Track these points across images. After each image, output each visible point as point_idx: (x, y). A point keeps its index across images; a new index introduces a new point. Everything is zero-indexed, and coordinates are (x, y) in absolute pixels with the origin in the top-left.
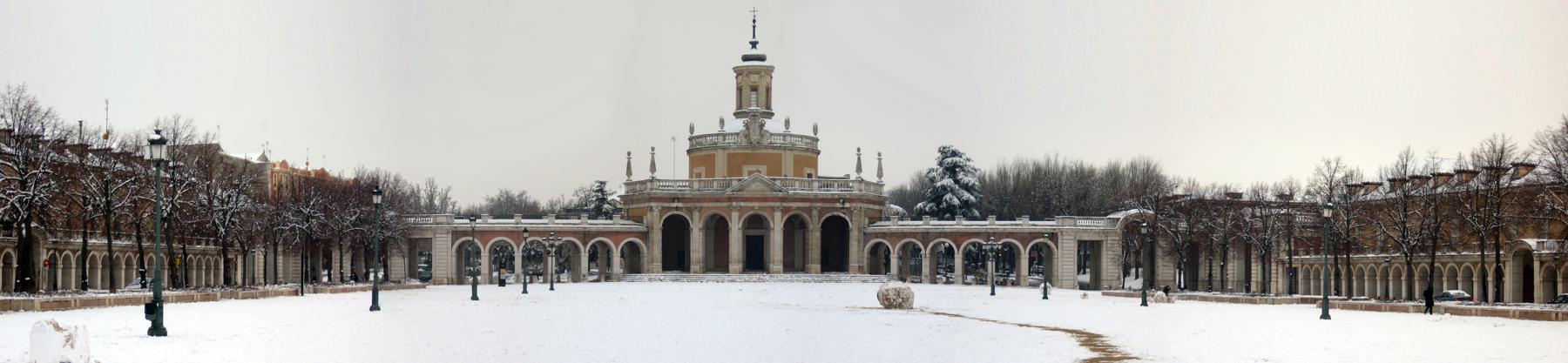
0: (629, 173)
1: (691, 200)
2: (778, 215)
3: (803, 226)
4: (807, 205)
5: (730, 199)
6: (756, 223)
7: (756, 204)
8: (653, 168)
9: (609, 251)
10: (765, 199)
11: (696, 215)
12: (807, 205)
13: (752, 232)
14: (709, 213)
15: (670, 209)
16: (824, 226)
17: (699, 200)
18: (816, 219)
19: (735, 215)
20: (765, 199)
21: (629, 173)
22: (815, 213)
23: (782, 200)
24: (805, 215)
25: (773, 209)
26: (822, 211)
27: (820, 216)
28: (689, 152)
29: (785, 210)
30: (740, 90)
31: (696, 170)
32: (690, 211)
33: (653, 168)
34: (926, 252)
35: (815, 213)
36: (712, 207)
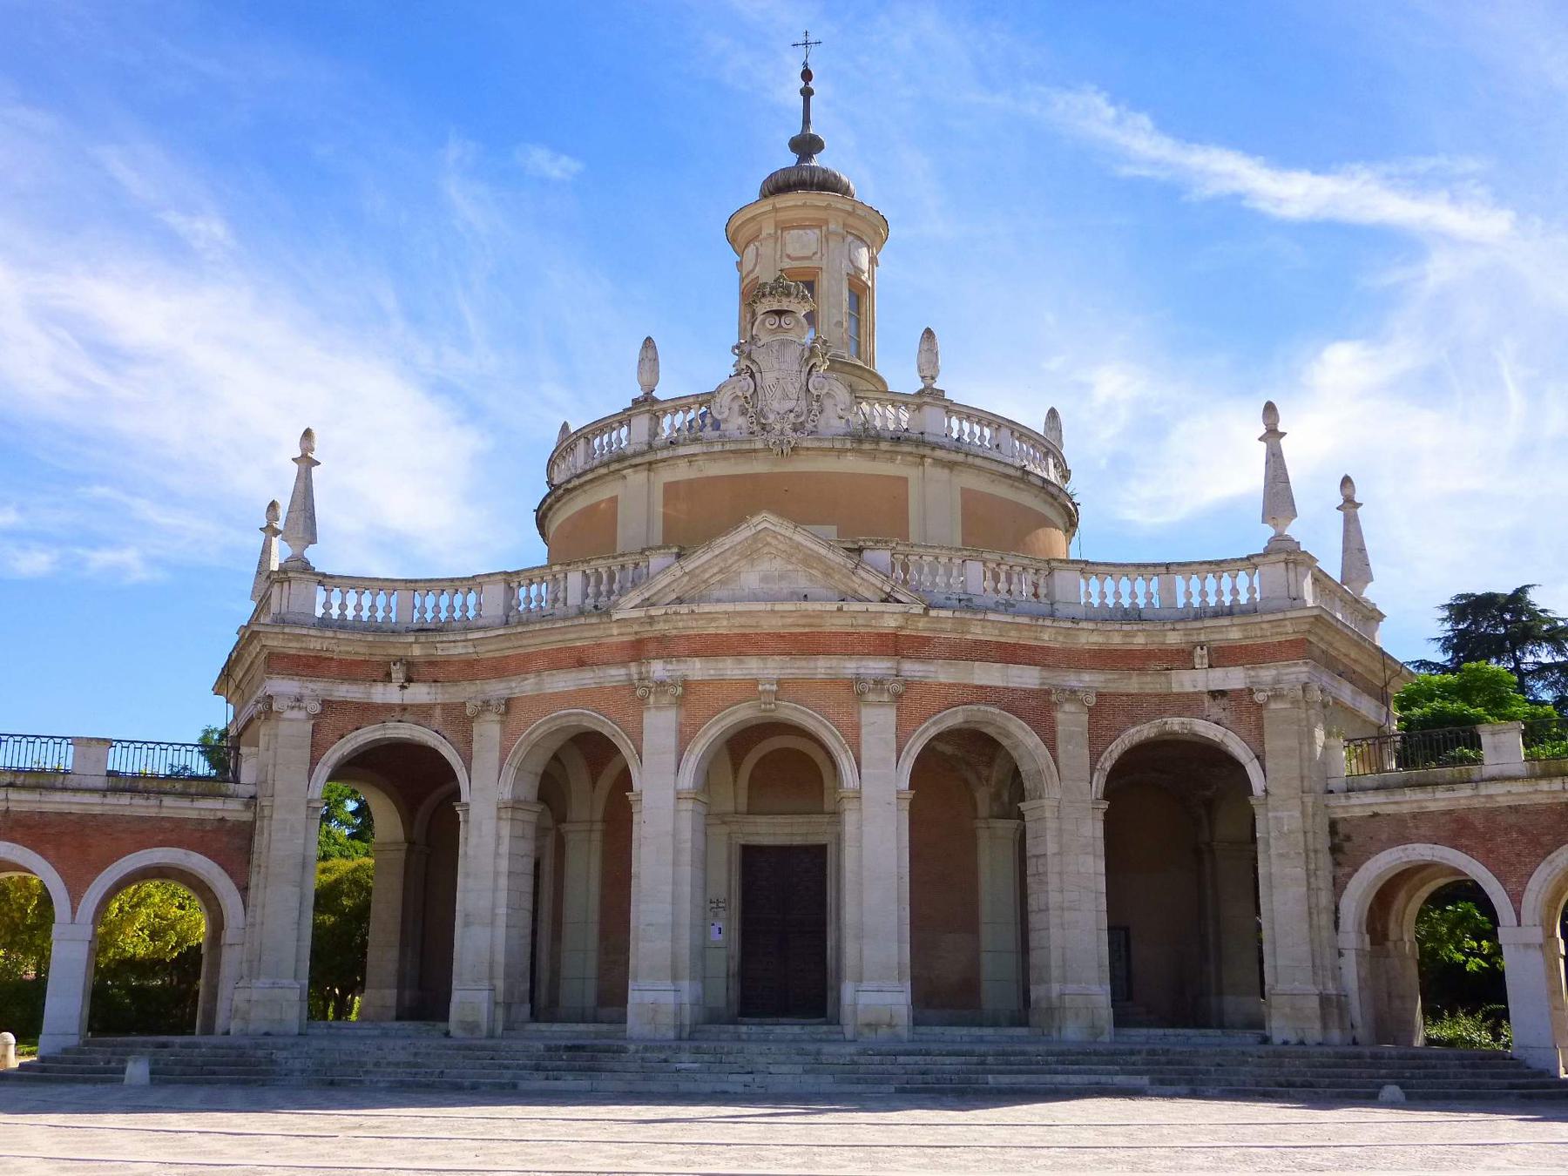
1: (470, 669)
2: (878, 721)
3: (1015, 792)
4: (1026, 677)
5: (638, 650)
6: (776, 764)
7: (766, 669)
10: (807, 644)
12: (1026, 677)
13: (773, 831)
14: (537, 727)
15: (369, 712)
16: (1113, 790)
17: (501, 669)
18: (1075, 750)
19: (660, 725)
20: (807, 644)
22: (1071, 721)
23: (894, 645)
24: (1023, 739)
25: (856, 689)
27: (1097, 742)
32: (460, 721)
35: (1071, 721)
36: (562, 695)
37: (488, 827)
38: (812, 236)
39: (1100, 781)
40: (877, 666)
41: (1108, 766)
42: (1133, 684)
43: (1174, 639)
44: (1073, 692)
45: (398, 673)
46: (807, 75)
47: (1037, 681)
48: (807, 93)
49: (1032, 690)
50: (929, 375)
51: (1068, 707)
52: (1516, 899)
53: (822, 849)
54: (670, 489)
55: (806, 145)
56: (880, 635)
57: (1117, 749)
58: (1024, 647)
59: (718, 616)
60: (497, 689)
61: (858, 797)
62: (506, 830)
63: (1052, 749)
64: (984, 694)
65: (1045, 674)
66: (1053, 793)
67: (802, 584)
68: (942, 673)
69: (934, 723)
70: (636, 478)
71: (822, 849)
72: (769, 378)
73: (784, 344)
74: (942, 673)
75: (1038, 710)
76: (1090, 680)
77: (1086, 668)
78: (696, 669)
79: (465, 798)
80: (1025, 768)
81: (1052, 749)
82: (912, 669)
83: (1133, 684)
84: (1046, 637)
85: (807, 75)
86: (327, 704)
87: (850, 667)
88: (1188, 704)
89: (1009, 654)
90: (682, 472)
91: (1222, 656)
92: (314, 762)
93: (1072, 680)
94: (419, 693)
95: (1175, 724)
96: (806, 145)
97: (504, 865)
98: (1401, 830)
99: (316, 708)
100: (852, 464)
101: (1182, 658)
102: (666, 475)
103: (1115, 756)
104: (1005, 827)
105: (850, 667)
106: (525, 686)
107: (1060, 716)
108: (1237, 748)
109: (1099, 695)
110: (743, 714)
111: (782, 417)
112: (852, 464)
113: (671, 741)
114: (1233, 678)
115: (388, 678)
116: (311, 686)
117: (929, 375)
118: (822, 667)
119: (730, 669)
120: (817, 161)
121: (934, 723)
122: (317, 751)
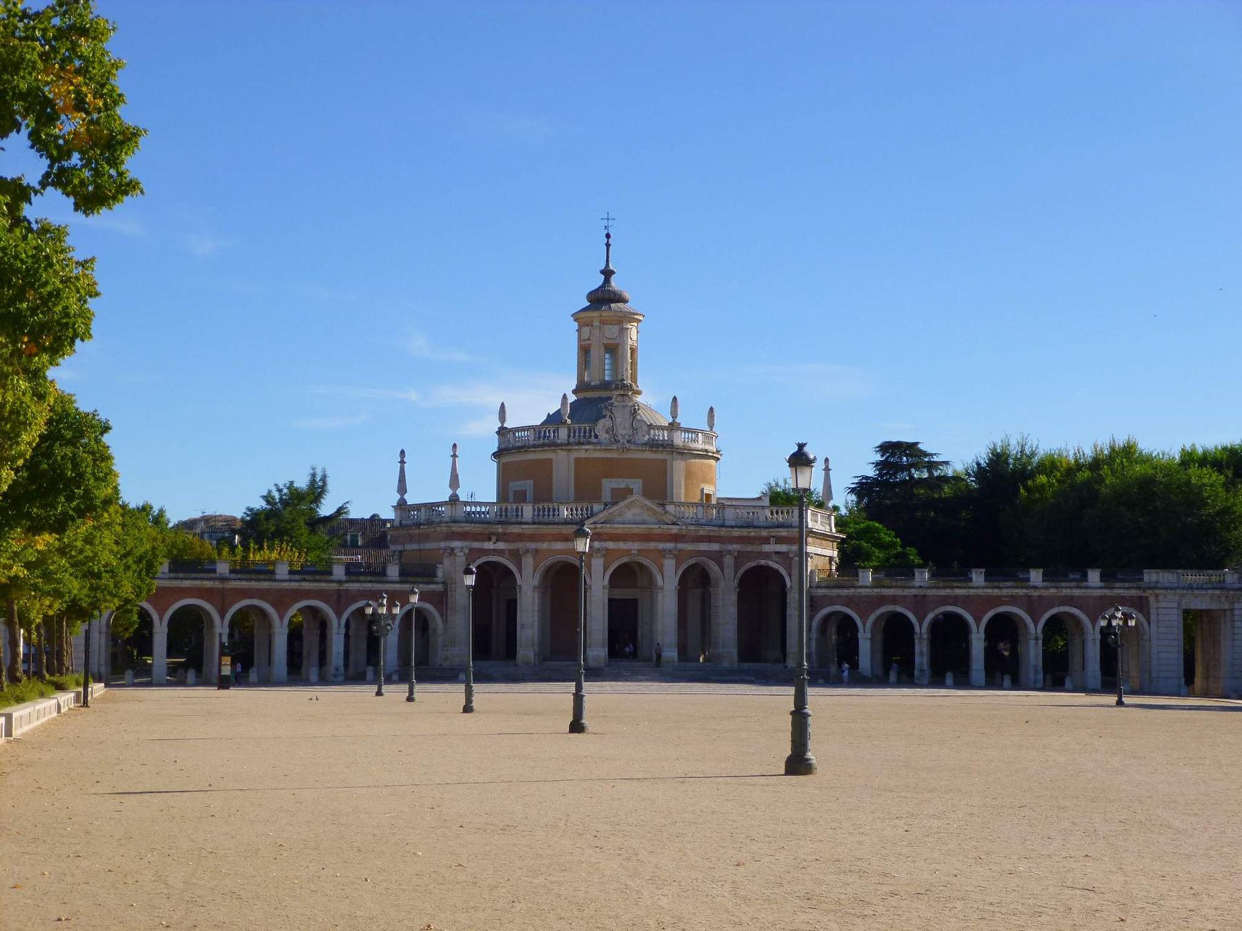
0: (402, 488)
2: (669, 564)
4: (715, 547)
6: (628, 575)
7: (634, 546)
8: (454, 481)
9: (323, 625)
11: (528, 562)
12: (715, 547)
13: (621, 594)
16: (742, 583)
17: (532, 538)
18: (729, 571)
20: (647, 537)
21: (402, 488)
22: (728, 561)
24: (714, 567)
25: (663, 553)
26: (740, 558)
27: (737, 566)
28: (496, 455)
29: (679, 556)
30: (584, 351)
31: (515, 486)
32: (516, 556)
33: (454, 481)
34: (922, 629)
35: (728, 561)
37: (530, 593)
38: (615, 328)
39: (737, 581)
40: (670, 545)
42: (749, 548)
43: (764, 533)
45: (494, 538)
46: (608, 236)
48: (608, 245)
50: (674, 414)
52: (864, 625)
53: (636, 600)
54: (577, 460)
55: (607, 273)
57: (742, 571)
59: (619, 529)
60: (532, 545)
61: (662, 588)
62: (536, 596)
63: (722, 570)
66: (722, 585)
67: (646, 517)
68: (689, 547)
70: (562, 454)
71: (636, 600)
72: (618, 420)
73: (624, 407)
74: (689, 547)
75: (718, 557)
78: (611, 545)
79: (519, 582)
80: (712, 576)
81: (722, 570)
82: (681, 546)
83: (749, 548)
85: (608, 236)
86: (470, 550)
87: (661, 546)
88: (767, 555)
89: (709, 539)
90: (583, 455)
91: (779, 540)
93: (730, 547)
94: (501, 545)
95: (763, 562)
96: (607, 273)
97: (536, 608)
98: (832, 600)
99: (467, 551)
100: (649, 455)
101: (766, 540)
102: (575, 455)
104: (698, 591)
105: (661, 546)
106: (545, 546)
108: (783, 571)
110: (625, 560)
111: (623, 437)
112: (649, 455)
113: (601, 569)
114: (783, 548)
115: (490, 539)
117: (674, 414)
118: (652, 545)
119: (622, 545)
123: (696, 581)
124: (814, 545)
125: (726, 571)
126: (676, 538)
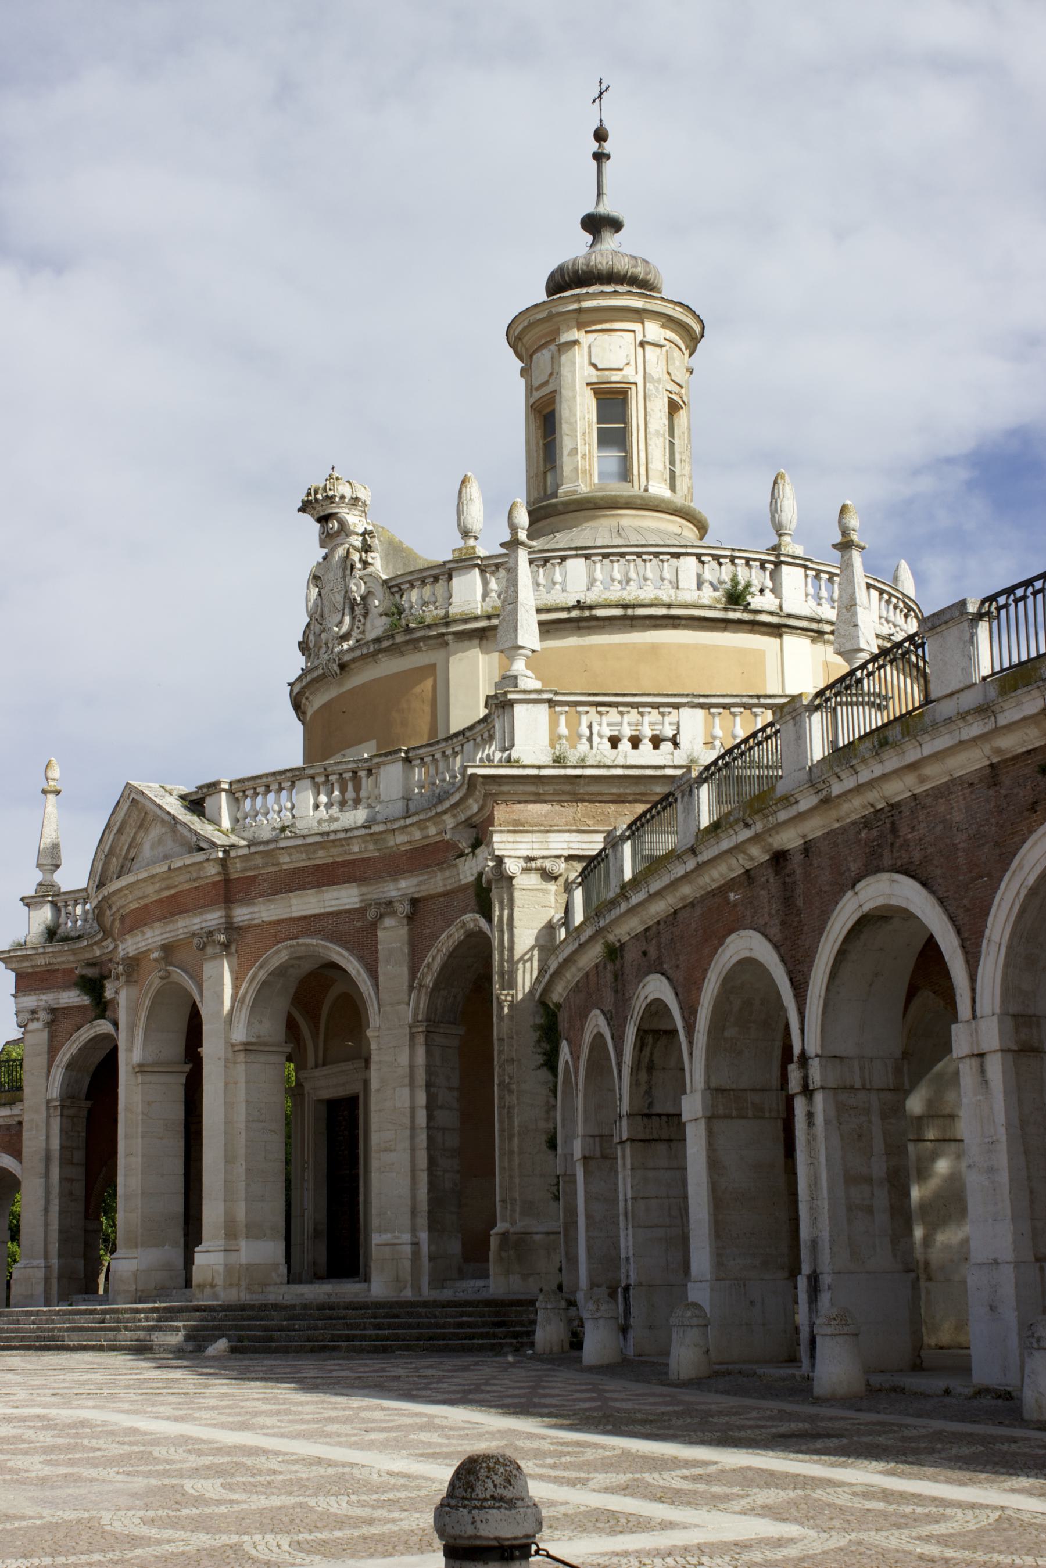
4: (344, 897)
12: (344, 897)
13: (329, 1083)
18: (394, 971)
22: (392, 935)
35: (392, 935)
40: (213, 918)
41: (429, 981)
44: (389, 903)
46: (600, 136)
47: (357, 899)
48: (600, 157)
49: (356, 910)
51: (388, 922)
56: (214, 884)
57: (436, 958)
58: (344, 864)
64: (308, 924)
65: (364, 890)
69: (261, 967)
75: (359, 930)
76: (406, 886)
77: (405, 872)
82: (242, 914)
84: (356, 849)
85: (600, 136)
86: (53, 1011)
92: (50, 1066)
99: (44, 1016)
103: (436, 966)
107: (380, 934)
109: (414, 902)
116: (44, 997)
120: (611, 242)
121: (261, 967)
122: (52, 1051)
123: (316, 1011)
124: (518, 828)
125: (384, 970)
126: (230, 888)
